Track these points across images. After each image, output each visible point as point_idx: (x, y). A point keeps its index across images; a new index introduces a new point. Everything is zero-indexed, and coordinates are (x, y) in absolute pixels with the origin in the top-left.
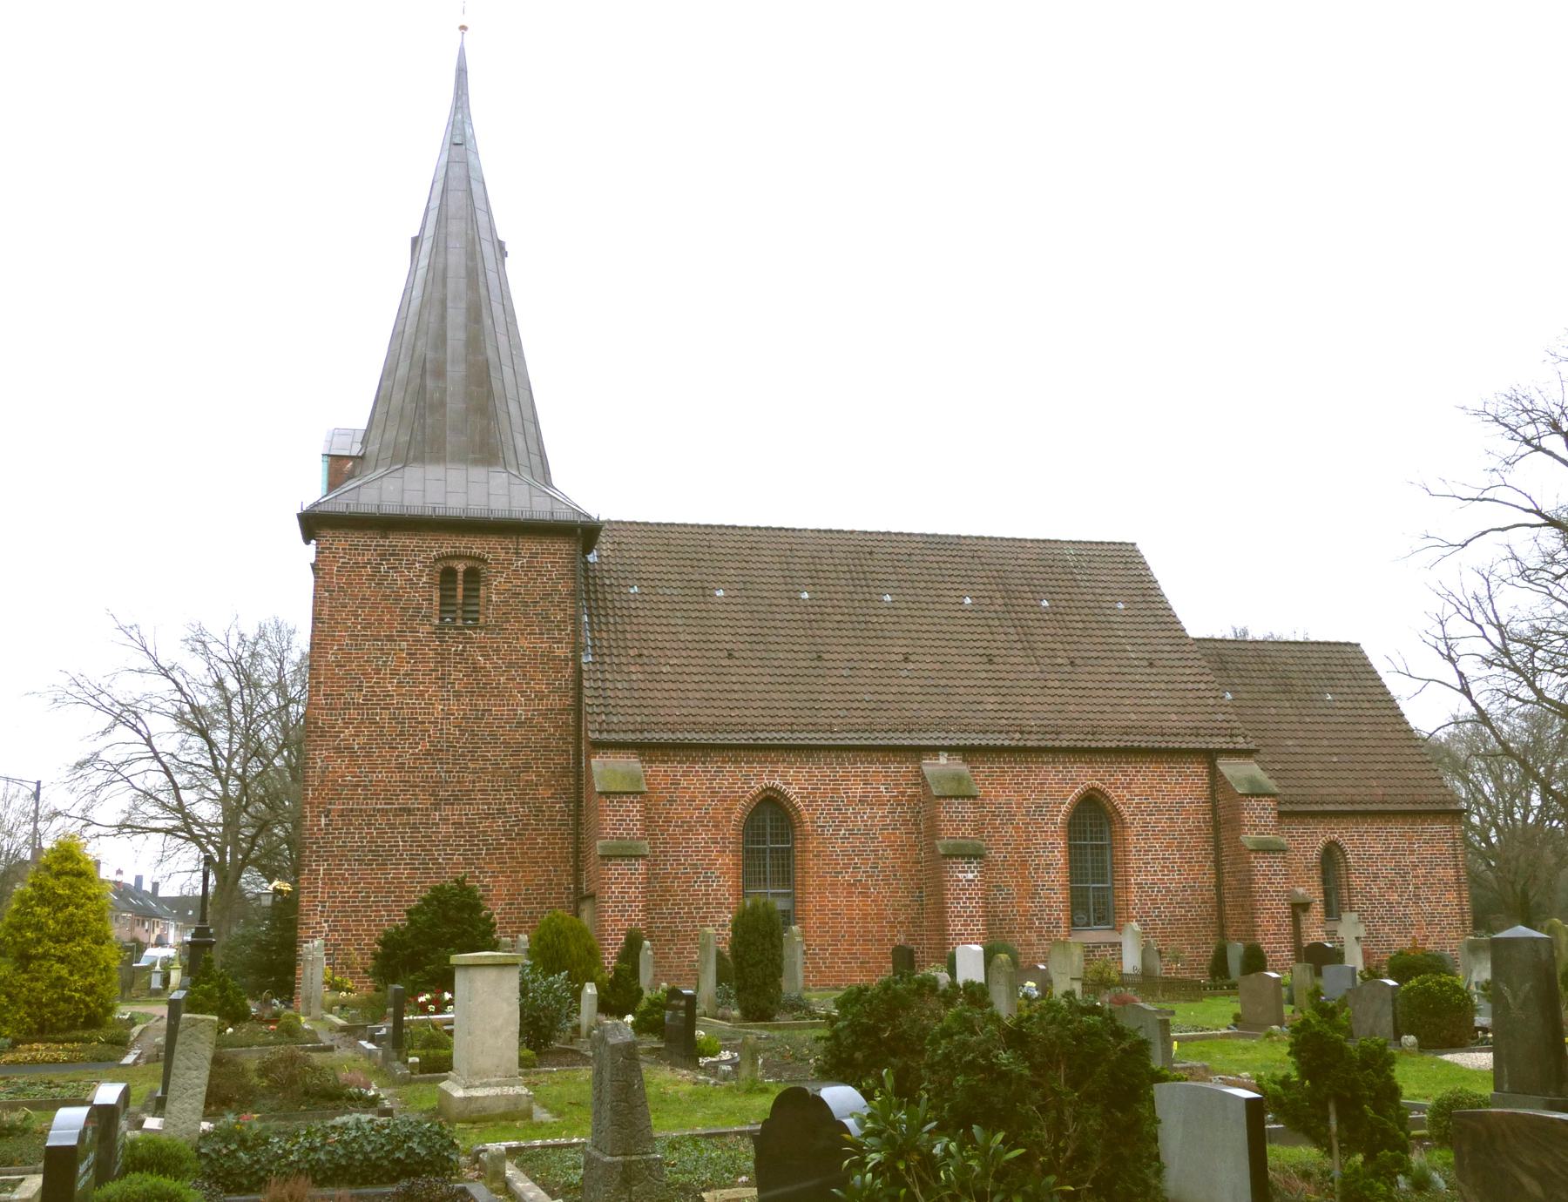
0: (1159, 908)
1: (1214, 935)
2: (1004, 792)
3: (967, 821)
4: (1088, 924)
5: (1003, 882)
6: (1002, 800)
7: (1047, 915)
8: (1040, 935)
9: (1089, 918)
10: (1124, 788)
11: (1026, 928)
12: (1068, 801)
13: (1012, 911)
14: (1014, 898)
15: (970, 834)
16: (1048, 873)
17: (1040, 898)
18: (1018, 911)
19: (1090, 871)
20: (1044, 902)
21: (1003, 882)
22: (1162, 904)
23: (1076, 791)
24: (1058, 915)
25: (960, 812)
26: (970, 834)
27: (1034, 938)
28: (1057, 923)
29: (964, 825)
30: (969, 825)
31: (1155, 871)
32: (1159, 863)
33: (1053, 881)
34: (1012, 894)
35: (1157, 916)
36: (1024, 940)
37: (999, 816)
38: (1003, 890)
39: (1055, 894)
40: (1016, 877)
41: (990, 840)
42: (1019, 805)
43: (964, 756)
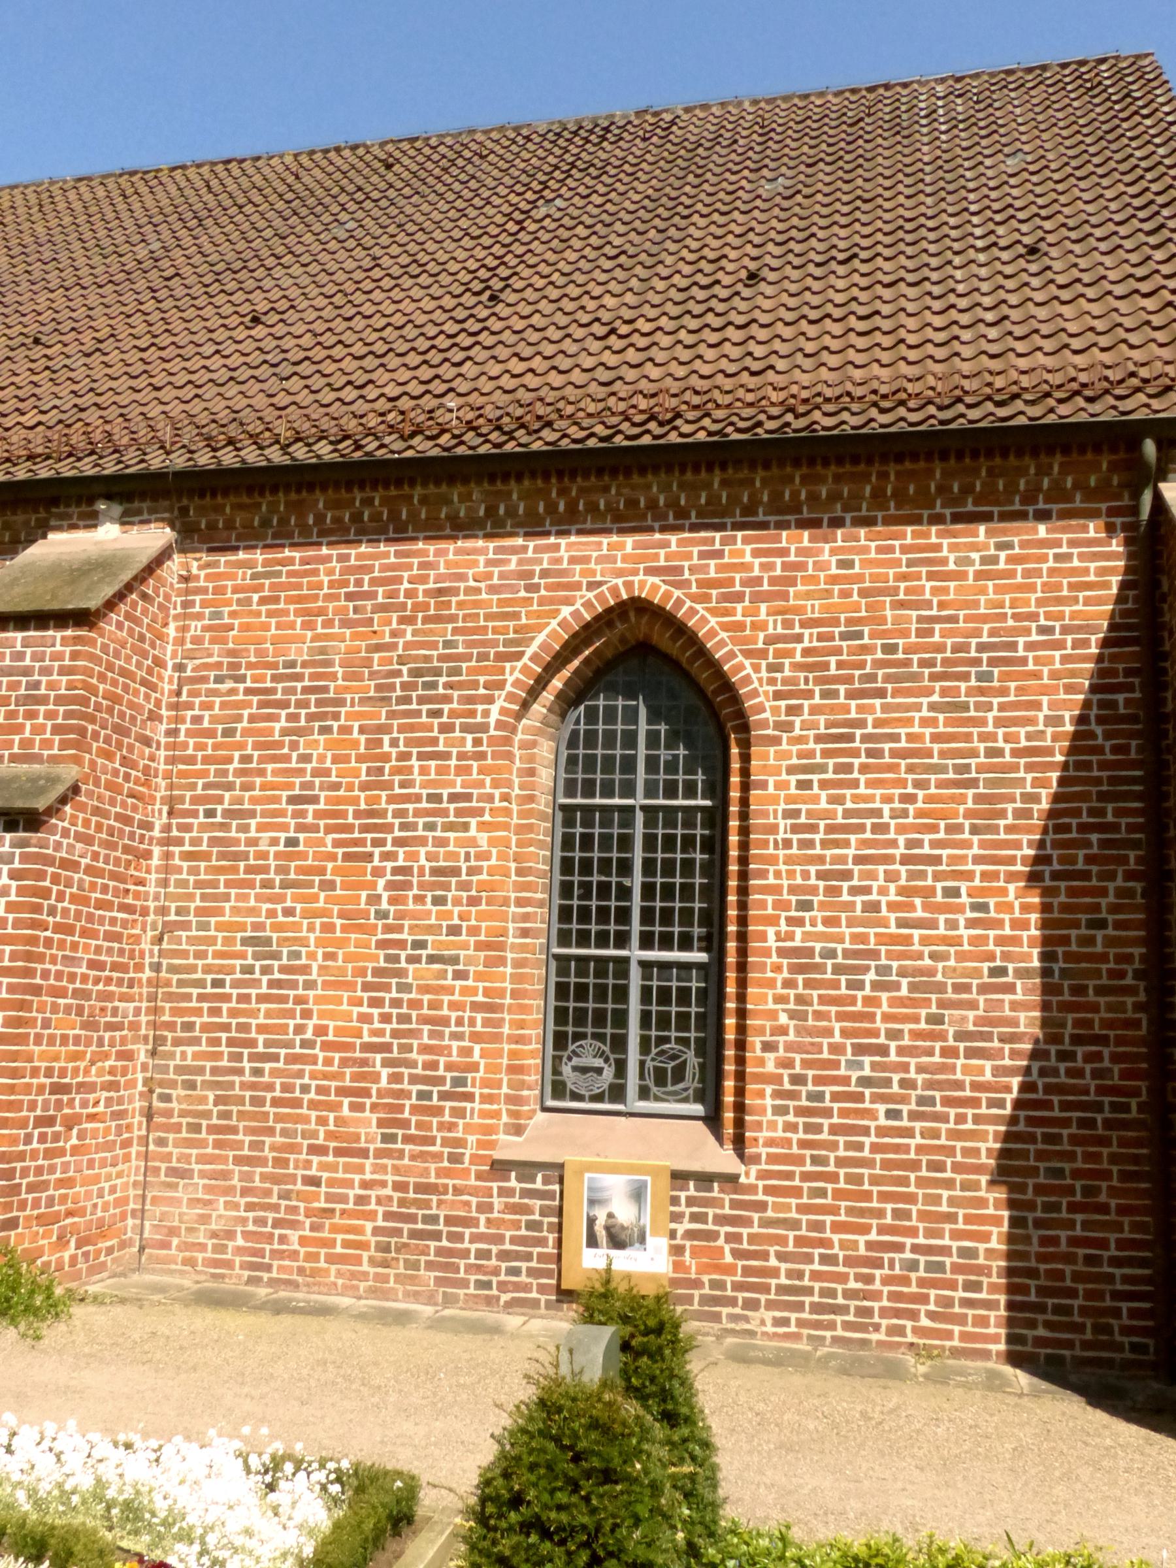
0: (883, 1051)
1: (1125, 1176)
2: (307, 626)
3: (43, 700)
4: (617, 1093)
5: (277, 927)
6: (300, 652)
7: (425, 1049)
8: (391, 1122)
9: (621, 1069)
10: (757, 598)
11: (342, 1092)
12: (529, 652)
13: (299, 1029)
14: (310, 985)
15: (46, 744)
16: (439, 901)
17: (404, 988)
18: (321, 1031)
19: (637, 902)
20: (415, 1004)
21: (277, 927)
22: (894, 1035)
23: (566, 611)
24: (466, 1052)
25: (27, 671)
26: (46, 744)
27: (368, 1127)
28: (459, 1082)
29: (31, 715)
30: (50, 715)
31: (874, 907)
32: (891, 877)
33: (454, 930)
34: (305, 969)
35: (864, 1081)
36: (330, 1135)
37: (285, 705)
38: (276, 956)
39: (459, 975)
40: (324, 913)
41: (247, 787)
42: (355, 667)
43: (184, 511)
